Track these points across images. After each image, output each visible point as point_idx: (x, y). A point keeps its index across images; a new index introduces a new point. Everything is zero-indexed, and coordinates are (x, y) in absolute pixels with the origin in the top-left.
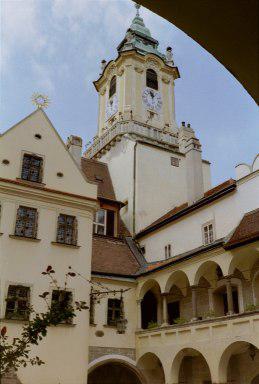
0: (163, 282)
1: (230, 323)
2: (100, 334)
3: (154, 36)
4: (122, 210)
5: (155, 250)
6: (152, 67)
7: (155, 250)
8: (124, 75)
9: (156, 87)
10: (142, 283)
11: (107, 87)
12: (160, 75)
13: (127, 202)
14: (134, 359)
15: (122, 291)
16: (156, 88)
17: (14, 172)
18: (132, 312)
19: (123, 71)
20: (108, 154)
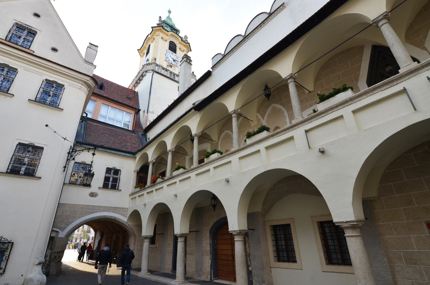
0: (151, 153)
1: (192, 174)
2: (93, 195)
3: (177, 27)
6: (173, 40)
8: (154, 42)
9: (175, 52)
10: (138, 156)
11: (146, 52)
12: (178, 46)
14: (126, 217)
16: (175, 52)
19: (154, 39)
20: (139, 85)
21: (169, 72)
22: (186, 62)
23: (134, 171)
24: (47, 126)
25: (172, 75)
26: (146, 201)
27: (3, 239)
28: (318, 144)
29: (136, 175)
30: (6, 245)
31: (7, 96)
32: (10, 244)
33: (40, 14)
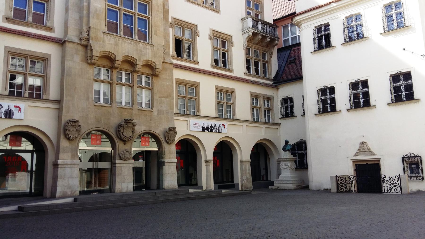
24: (404, 49)
27: (412, 154)
30: (416, 159)
31: (365, 40)
32: (419, 158)
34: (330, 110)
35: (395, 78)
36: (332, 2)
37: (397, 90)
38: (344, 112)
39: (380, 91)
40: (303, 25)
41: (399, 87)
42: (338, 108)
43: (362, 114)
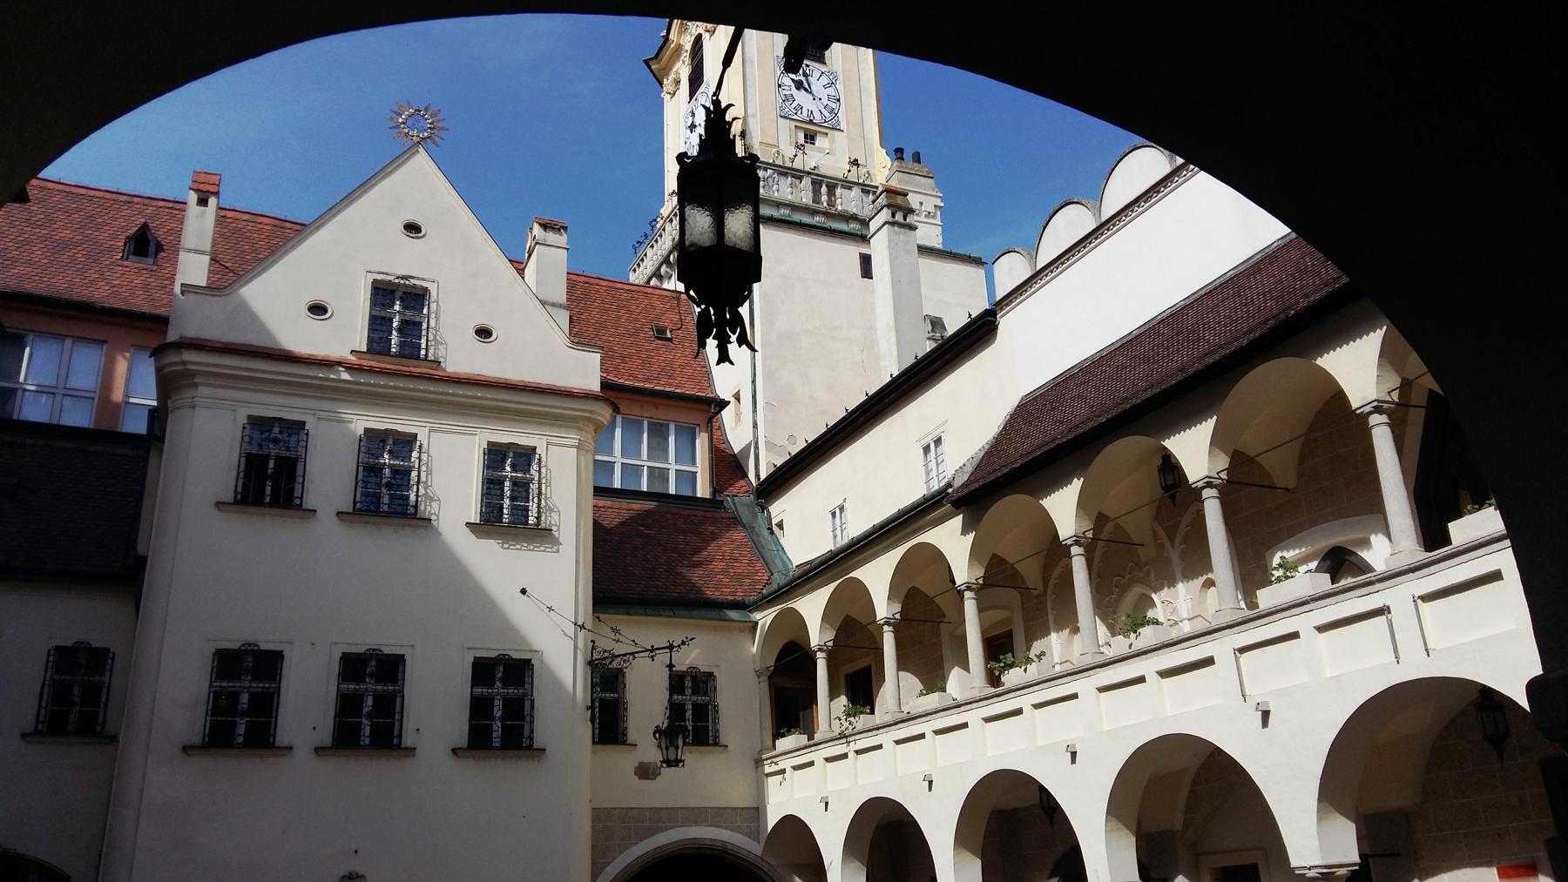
2: (645, 772)
4: (727, 414)
5: (805, 525)
7: (805, 525)
11: (683, 69)
13: (737, 397)
15: (671, 647)
17: (345, 335)
18: (741, 702)
21: (807, 181)
22: (892, 224)
23: (758, 674)
25: (824, 189)
26: (830, 789)
28: (1256, 692)
29: (765, 686)
33: (419, 221)
34: (240, 739)
35: (483, 670)
36: (339, 363)
37: (480, 708)
38: (303, 754)
39: (436, 704)
40: (202, 391)
41: (489, 701)
42: (284, 736)
43: (365, 776)
